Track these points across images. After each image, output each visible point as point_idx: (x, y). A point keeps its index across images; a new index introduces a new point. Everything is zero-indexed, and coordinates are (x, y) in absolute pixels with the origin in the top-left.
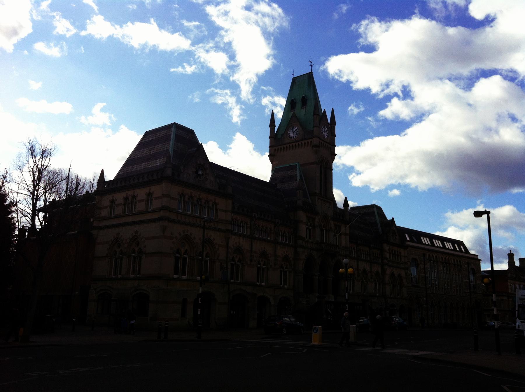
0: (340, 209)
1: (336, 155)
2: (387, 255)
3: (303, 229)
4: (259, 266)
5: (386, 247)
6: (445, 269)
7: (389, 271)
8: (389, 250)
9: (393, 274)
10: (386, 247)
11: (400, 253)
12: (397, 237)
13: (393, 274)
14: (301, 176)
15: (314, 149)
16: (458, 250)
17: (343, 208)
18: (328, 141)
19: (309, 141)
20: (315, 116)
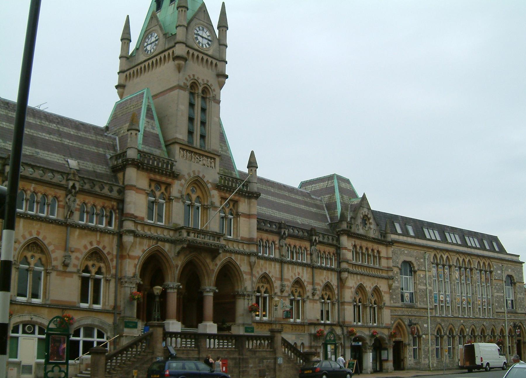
0: (241, 173)
1: (227, 77)
2: (349, 255)
3: (137, 204)
4: (258, 294)
5: (345, 241)
6: (463, 277)
7: (352, 282)
8: (355, 246)
9: (361, 288)
10: (345, 241)
11: (378, 252)
12: (372, 226)
13: (361, 288)
14: (149, 109)
15: (177, 62)
16: (488, 248)
17: (246, 171)
18: (210, 53)
19: (171, 51)
20: (180, 9)
